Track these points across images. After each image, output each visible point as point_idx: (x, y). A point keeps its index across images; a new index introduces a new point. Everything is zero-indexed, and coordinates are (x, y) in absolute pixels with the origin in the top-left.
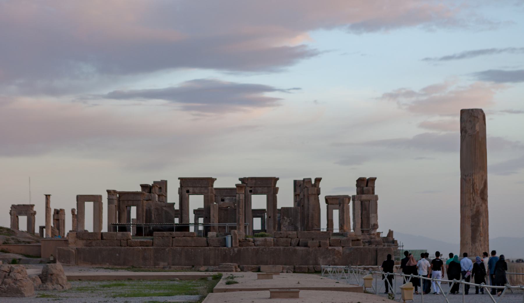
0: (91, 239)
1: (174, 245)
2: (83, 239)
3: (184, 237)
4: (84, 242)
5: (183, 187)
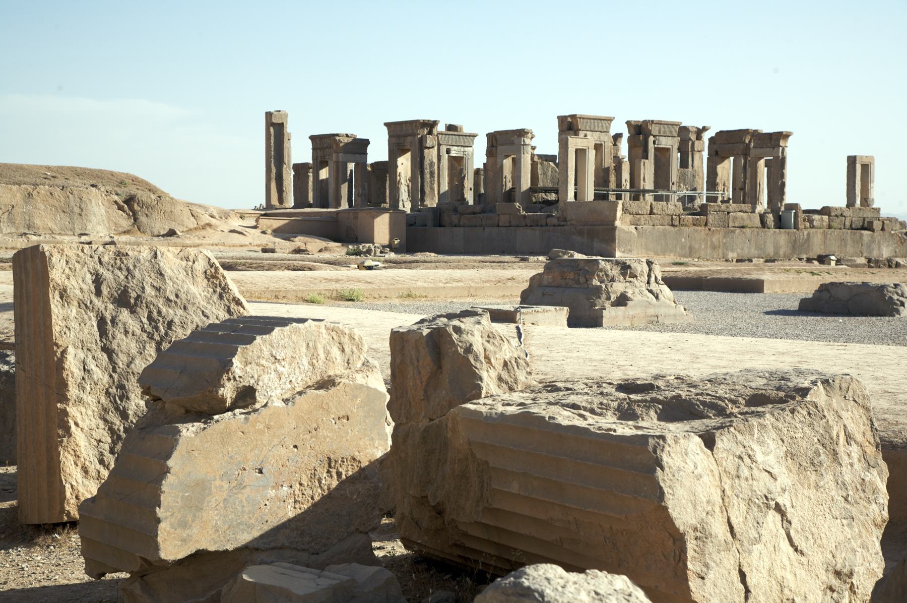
0: (640, 213)
1: (730, 226)
2: (630, 214)
3: (741, 213)
4: (631, 217)
5: (580, 130)
